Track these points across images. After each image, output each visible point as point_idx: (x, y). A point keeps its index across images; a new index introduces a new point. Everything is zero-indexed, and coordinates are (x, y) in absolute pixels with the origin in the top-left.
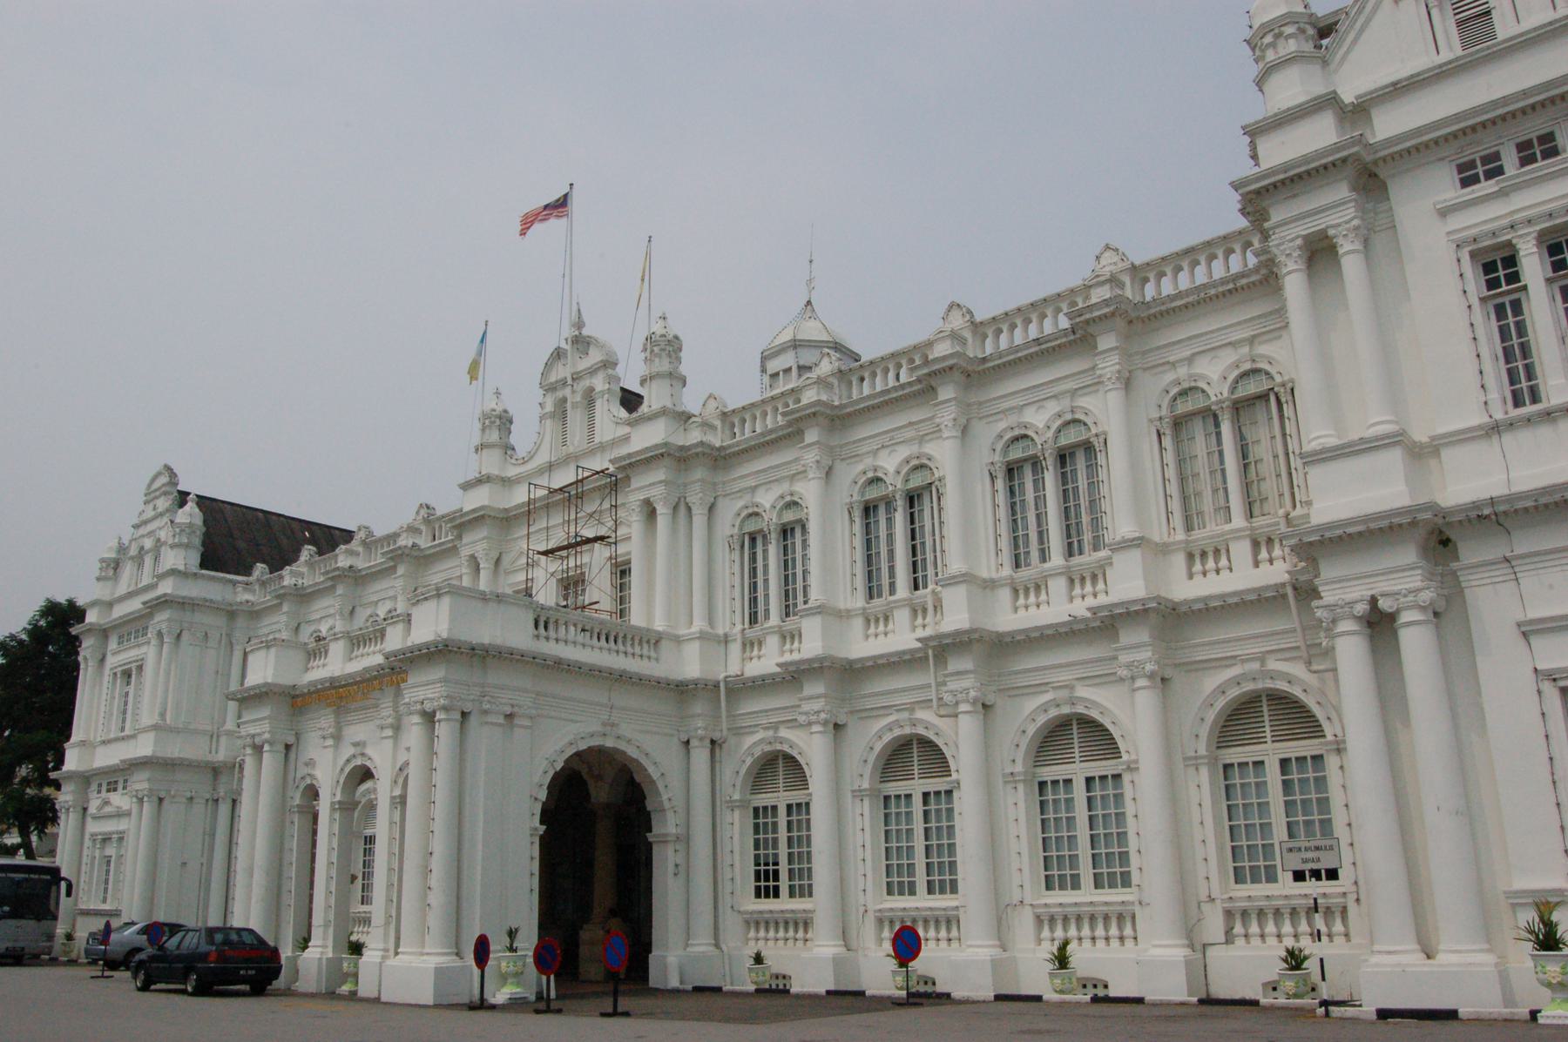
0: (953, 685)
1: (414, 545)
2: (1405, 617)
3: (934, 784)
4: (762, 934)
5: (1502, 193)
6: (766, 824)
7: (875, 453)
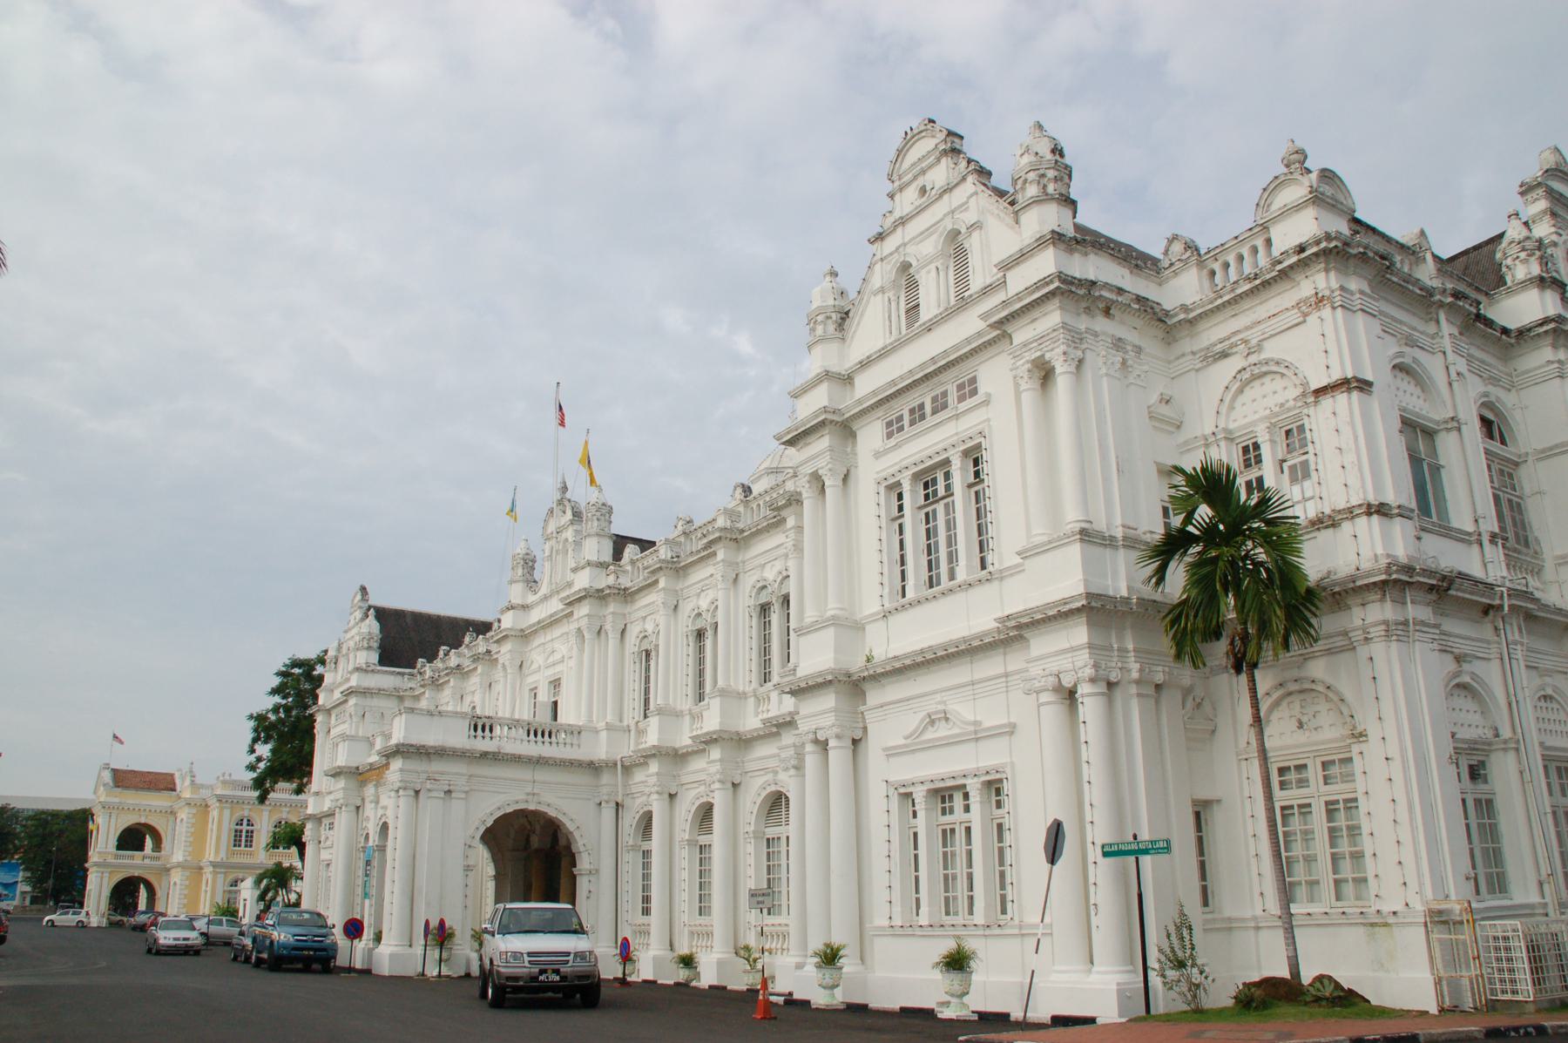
5: (897, 446)
7: (698, 595)
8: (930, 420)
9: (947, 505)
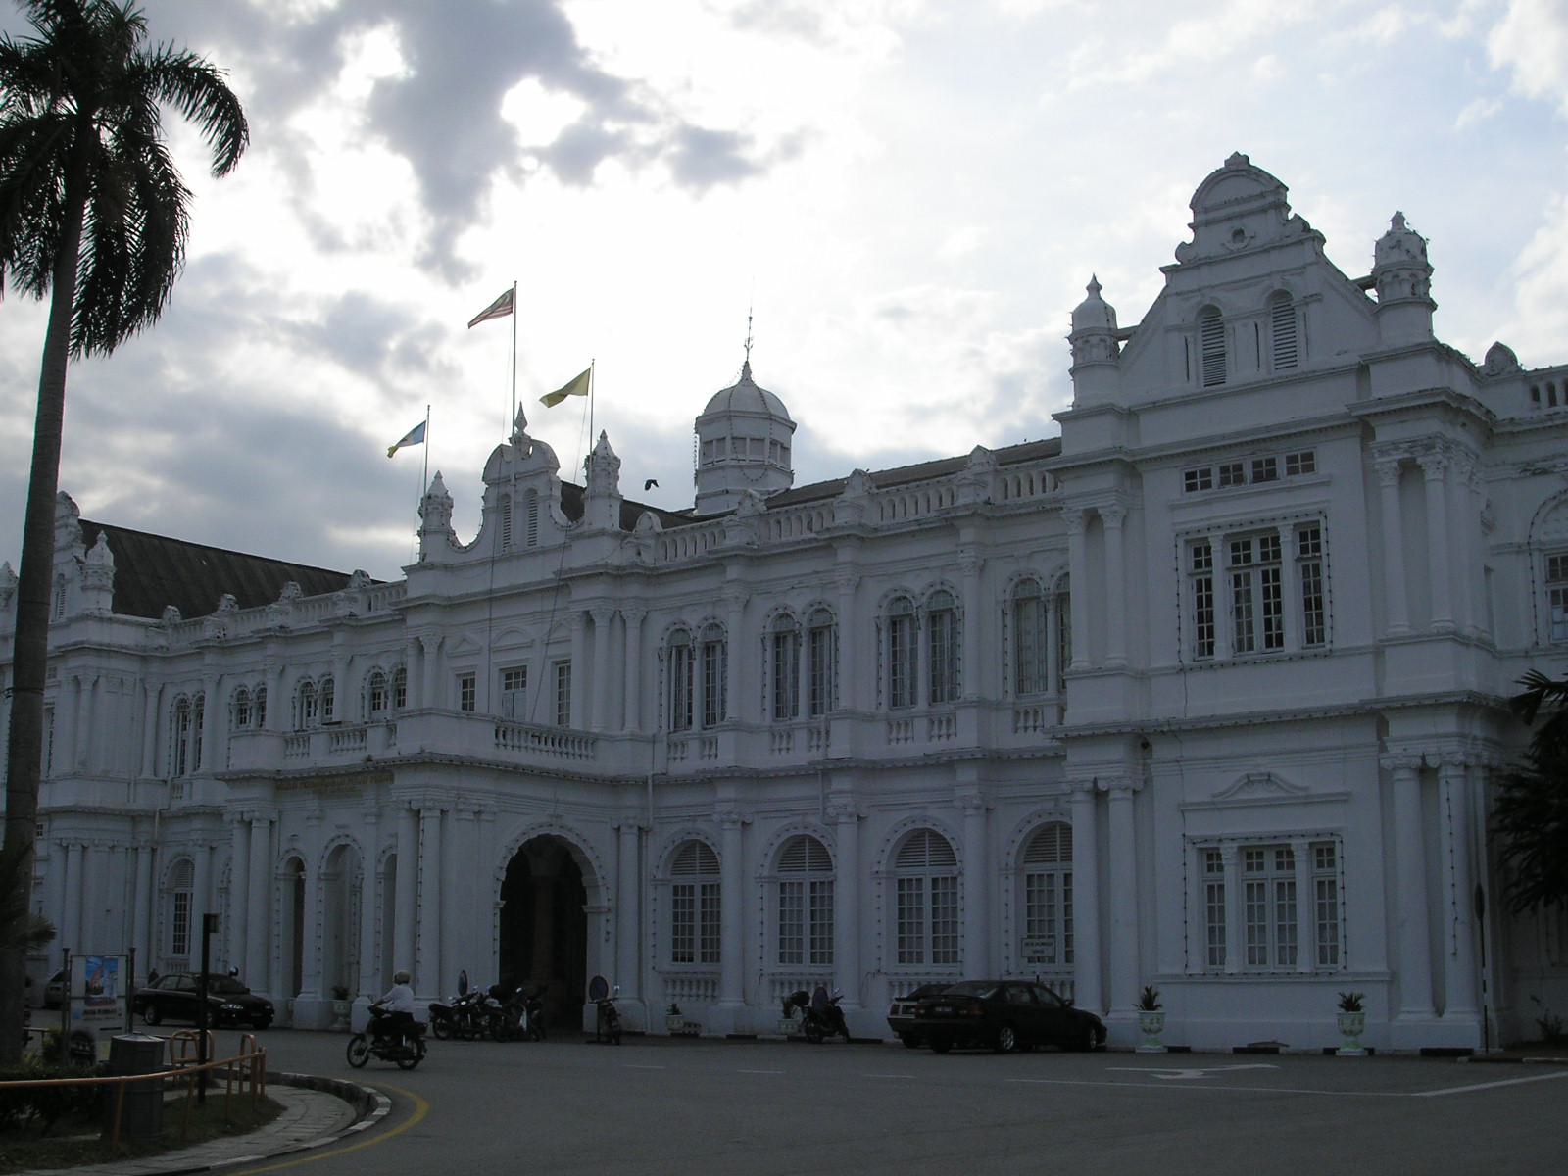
0: (836, 800)
1: (352, 615)
2: (1112, 795)
3: (819, 876)
4: (678, 990)
5: (1206, 502)
6: (683, 901)
8: (1248, 486)
9: (1265, 575)
